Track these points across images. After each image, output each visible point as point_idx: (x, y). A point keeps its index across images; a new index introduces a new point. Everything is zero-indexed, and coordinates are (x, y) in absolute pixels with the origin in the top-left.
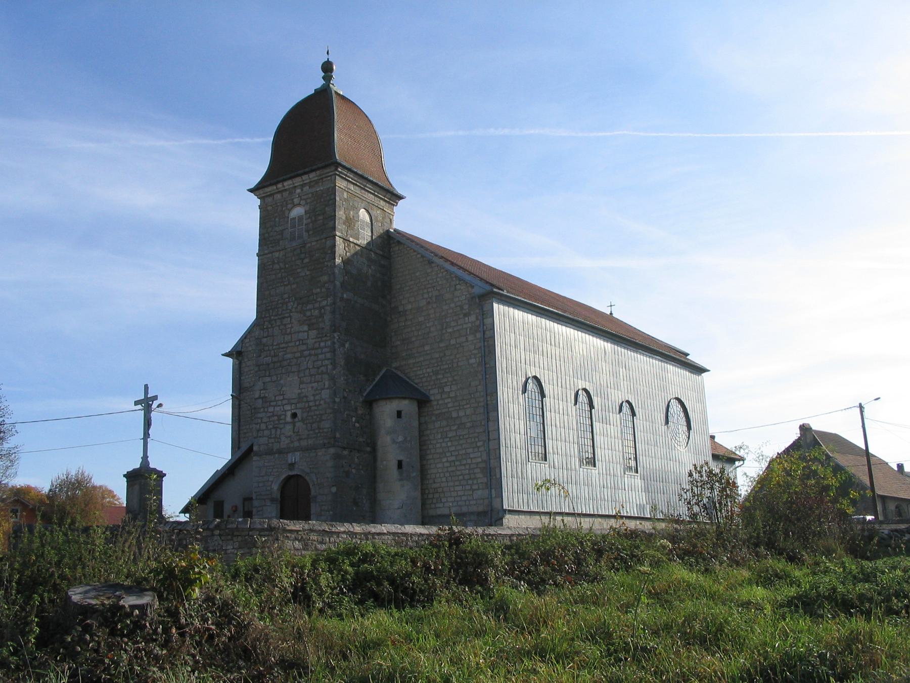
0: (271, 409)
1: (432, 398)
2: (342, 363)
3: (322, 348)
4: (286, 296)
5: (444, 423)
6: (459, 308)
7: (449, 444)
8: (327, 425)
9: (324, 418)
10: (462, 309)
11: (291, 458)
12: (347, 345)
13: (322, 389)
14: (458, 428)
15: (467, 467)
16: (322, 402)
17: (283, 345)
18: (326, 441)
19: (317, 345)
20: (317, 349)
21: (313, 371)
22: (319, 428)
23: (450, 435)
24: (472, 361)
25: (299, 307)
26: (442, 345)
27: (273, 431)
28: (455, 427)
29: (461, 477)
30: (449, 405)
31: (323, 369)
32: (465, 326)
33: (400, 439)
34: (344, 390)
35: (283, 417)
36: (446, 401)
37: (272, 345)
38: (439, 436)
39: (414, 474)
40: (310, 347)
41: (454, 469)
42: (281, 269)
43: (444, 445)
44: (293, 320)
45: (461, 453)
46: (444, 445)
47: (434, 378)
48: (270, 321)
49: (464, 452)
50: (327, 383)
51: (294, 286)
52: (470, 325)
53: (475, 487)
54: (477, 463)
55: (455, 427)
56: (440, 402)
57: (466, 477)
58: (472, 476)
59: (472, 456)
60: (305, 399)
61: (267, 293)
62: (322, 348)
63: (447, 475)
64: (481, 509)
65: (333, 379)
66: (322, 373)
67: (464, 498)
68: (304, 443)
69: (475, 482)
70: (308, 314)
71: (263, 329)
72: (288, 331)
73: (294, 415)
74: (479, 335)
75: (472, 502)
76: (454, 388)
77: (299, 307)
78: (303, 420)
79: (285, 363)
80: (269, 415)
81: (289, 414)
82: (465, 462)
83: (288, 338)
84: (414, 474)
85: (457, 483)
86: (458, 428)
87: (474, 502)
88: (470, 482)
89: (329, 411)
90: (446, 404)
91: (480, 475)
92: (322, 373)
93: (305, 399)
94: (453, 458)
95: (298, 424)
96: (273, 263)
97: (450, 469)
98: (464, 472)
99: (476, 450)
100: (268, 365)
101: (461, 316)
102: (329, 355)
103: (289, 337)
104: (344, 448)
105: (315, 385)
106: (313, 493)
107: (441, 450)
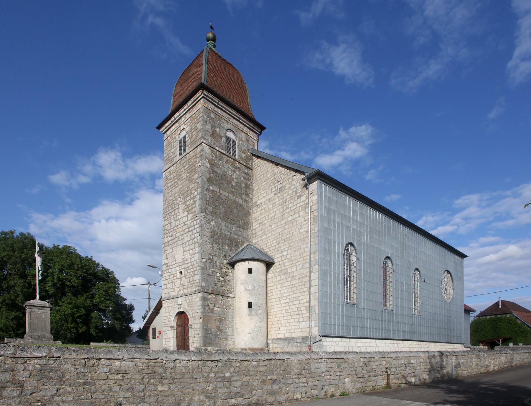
0: (170, 271)
1: (275, 261)
2: (208, 235)
3: (194, 226)
4: (177, 194)
5: (283, 277)
7: (286, 291)
8: (197, 277)
9: (196, 273)
11: (180, 300)
12: (213, 223)
13: (195, 254)
14: (292, 280)
17: (176, 228)
18: (197, 289)
19: (192, 224)
21: (190, 242)
23: (286, 284)
26: (283, 222)
28: (289, 279)
29: (292, 313)
30: (286, 264)
31: (195, 240)
33: (250, 287)
34: (209, 254)
35: (175, 275)
36: (285, 261)
38: (279, 286)
39: (260, 311)
40: (189, 226)
41: (288, 308)
42: (174, 177)
45: (293, 296)
46: (282, 292)
47: (277, 246)
49: (295, 296)
50: (197, 249)
53: (301, 320)
54: (303, 303)
56: (281, 263)
58: (300, 312)
59: (300, 298)
63: (284, 312)
64: (304, 335)
65: (201, 246)
66: (195, 242)
68: (186, 291)
69: (301, 316)
70: (188, 203)
73: (181, 273)
74: (307, 210)
76: (290, 251)
79: (176, 240)
81: (178, 272)
82: (295, 303)
84: (260, 311)
85: (290, 317)
86: (292, 280)
87: (300, 330)
88: (298, 316)
89: (198, 268)
90: (284, 263)
91: (304, 312)
92: (195, 242)
94: (288, 301)
95: (183, 279)
96: (171, 174)
97: (285, 308)
98: (294, 310)
99: (303, 294)
104: (210, 294)
105: (191, 251)
106: (190, 323)
107: (280, 296)
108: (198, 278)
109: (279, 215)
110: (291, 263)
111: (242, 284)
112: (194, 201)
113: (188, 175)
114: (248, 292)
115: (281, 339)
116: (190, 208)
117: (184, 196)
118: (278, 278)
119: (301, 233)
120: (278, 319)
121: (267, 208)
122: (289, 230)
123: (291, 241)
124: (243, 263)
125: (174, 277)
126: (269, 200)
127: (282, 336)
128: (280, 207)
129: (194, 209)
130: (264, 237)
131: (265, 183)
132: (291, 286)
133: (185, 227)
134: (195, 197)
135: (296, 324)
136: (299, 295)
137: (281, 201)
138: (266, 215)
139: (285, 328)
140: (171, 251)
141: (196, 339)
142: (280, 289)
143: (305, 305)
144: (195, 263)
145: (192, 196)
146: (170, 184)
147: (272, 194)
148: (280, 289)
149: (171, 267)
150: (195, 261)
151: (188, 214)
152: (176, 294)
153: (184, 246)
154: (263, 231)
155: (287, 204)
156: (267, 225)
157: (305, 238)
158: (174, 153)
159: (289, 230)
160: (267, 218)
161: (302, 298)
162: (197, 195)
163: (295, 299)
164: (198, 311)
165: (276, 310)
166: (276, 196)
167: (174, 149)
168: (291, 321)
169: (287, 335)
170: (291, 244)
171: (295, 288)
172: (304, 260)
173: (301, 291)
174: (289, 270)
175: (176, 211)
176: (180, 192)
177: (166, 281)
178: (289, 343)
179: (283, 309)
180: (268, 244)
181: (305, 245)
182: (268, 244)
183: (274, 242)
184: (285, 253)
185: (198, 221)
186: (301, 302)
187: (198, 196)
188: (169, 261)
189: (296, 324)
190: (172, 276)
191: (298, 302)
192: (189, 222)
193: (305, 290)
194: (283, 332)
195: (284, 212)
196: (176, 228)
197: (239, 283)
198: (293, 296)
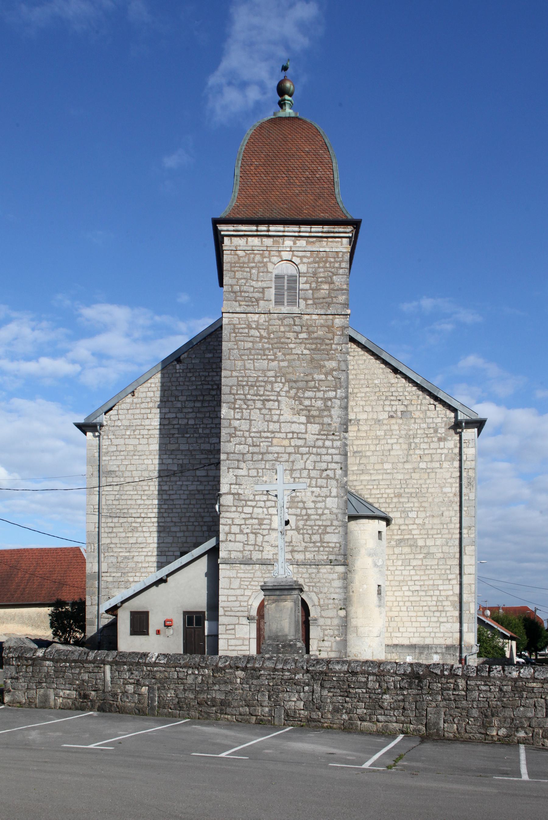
0: (248, 510)
4: (272, 373)
5: (407, 550)
6: (432, 431)
7: (413, 572)
9: (329, 529)
10: (436, 431)
13: (326, 497)
14: (425, 558)
15: (435, 598)
16: (327, 511)
17: (269, 435)
18: (331, 557)
19: (320, 443)
20: (319, 447)
21: (313, 474)
22: (321, 541)
23: (414, 563)
24: (447, 490)
25: (293, 392)
26: (407, 466)
27: (252, 536)
28: (421, 556)
29: (426, 608)
32: (439, 451)
35: (265, 522)
36: (411, 527)
37: (249, 431)
38: (400, 563)
43: (405, 573)
44: (283, 406)
45: (426, 583)
46: (405, 573)
48: (245, 401)
49: (431, 582)
50: (334, 492)
51: (285, 364)
52: (446, 451)
53: (441, 620)
54: (447, 596)
55: (421, 556)
56: (403, 527)
57: (435, 608)
58: (440, 608)
59: (441, 588)
60: (301, 505)
61: (239, 363)
62: (327, 448)
64: (449, 642)
67: (430, 630)
68: (299, 557)
69: (443, 614)
70: (307, 403)
71: (234, 409)
72: (275, 418)
75: (437, 635)
76: (422, 515)
77: (293, 392)
78: (297, 529)
79: (270, 457)
80: (243, 516)
82: (431, 593)
83: (272, 426)
85: (419, 614)
86: (425, 558)
87: (441, 635)
88: (437, 614)
90: (411, 530)
91: (450, 608)
92: (328, 478)
93: (301, 505)
94: (418, 588)
97: (412, 599)
98: (430, 603)
100: (243, 454)
101: (435, 439)
102: (337, 458)
103: (277, 426)
107: (401, 578)
108: (335, 540)
109: (400, 453)
110: (423, 532)
111: (370, 555)
112: (326, 406)
113: (306, 352)
114: (377, 570)
115: (402, 646)
116: (315, 413)
117: (294, 385)
118: (397, 550)
119: (445, 493)
120: (396, 614)
121: (372, 434)
122: (420, 482)
123: (425, 499)
124: (371, 521)
125: (260, 524)
126: (378, 421)
127: (406, 642)
128: (401, 440)
129: (327, 420)
130: (367, 477)
131: (368, 389)
132: (423, 567)
133: (301, 442)
134: (330, 399)
135: (434, 625)
136: (440, 582)
137: (403, 432)
138: (369, 442)
139: (409, 630)
140: (253, 473)
141: (326, 644)
142: (399, 568)
143: (451, 598)
144: (327, 511)
145: (320, 394)
146: (250, 345)
147: (386, 415)
148: (399, 568)
149: (249, 503)
150: (326, 508)
151: (308, 422)
152: (270, 557)
153: (296, 474)
154: (362, 467)
155: (417, 441)
156: (373, 459)
157: (451, 502)
158: (263, 292)
159: (420, 482)
160: (372, 448)
161: (445, 587)
162: (335, 398)
163: (430, 587)
164: (336, 596)
165: (393, 599)
166: (393, 421)
167: (264, 285)
168: (425, 619)
169: (414, 641)
170: (424, 504)
171: (433, 572)
172: (449, 533)
173: (445, 577)
174: (421, 543)
175: (269, 405)
176: (281, 373)
177: (235, 529)
178: (421, 653)
179: (407, 599)
180: (374, 492)
181: (452, 513)
182: (374, 492)
183: (388, 491)
184: (412, 515)
185: (338, 444)
186: (443, 593)
187: (338, 402)
188: (247, 491)
189: (434, 625)
190: (256, 521)
191: (437, 593)
192: (310, 438)
193: (450, 577)
194: (405, 635)
195: (411, 452)
196: (269, 435)
197: (363, 551)
198: (426, 583)
